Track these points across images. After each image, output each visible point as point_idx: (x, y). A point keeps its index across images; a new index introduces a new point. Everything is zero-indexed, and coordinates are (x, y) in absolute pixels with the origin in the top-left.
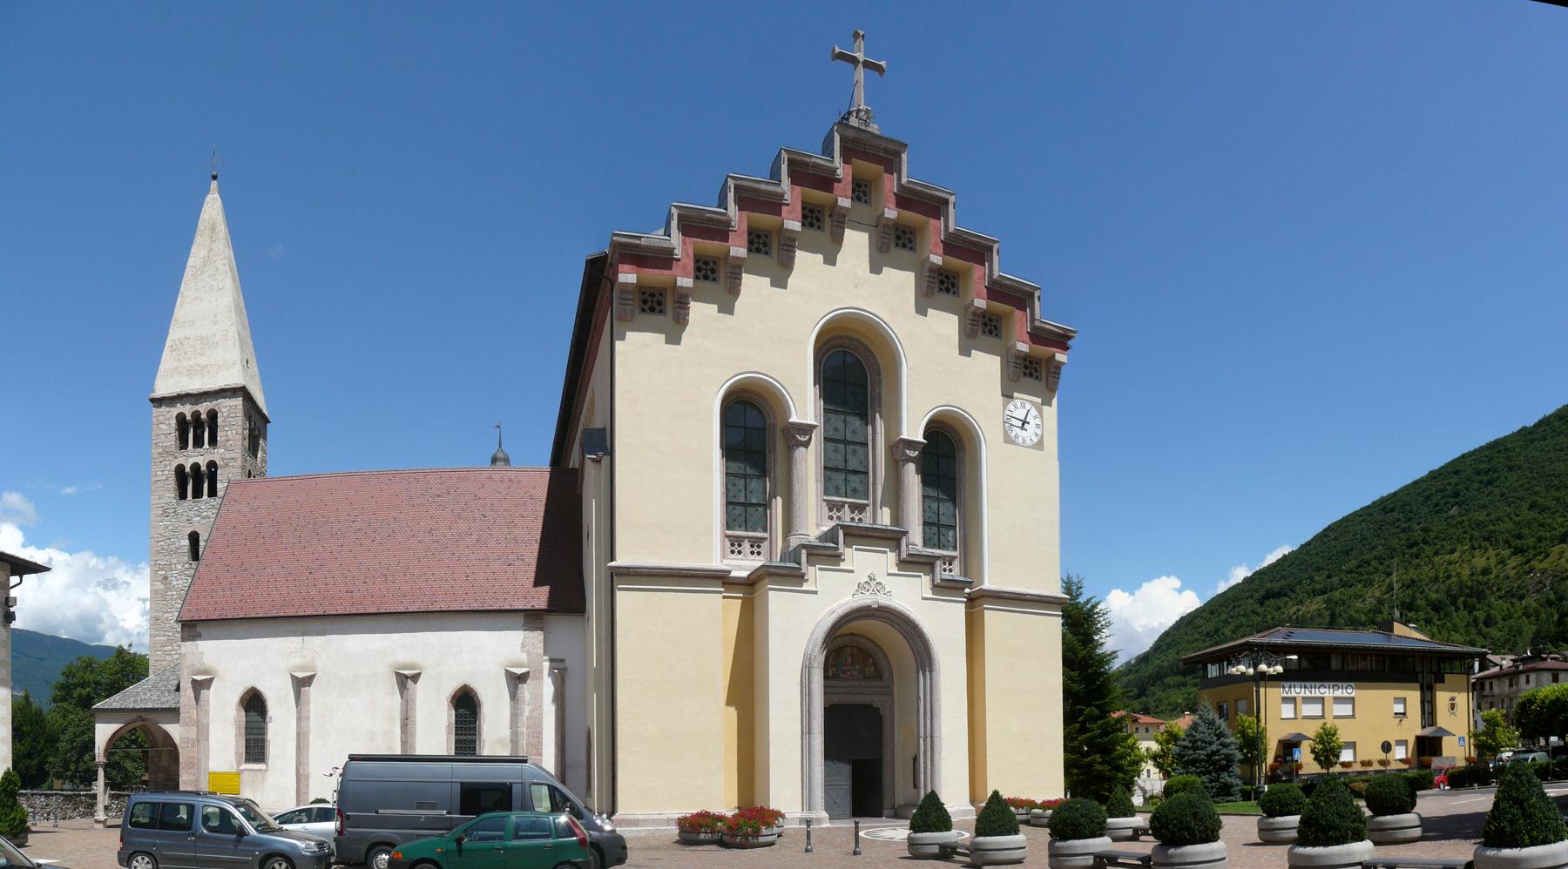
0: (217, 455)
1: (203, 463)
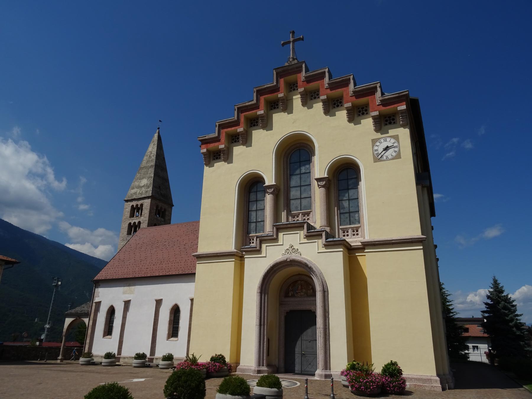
0: (141, 219)
1: (137, 221)
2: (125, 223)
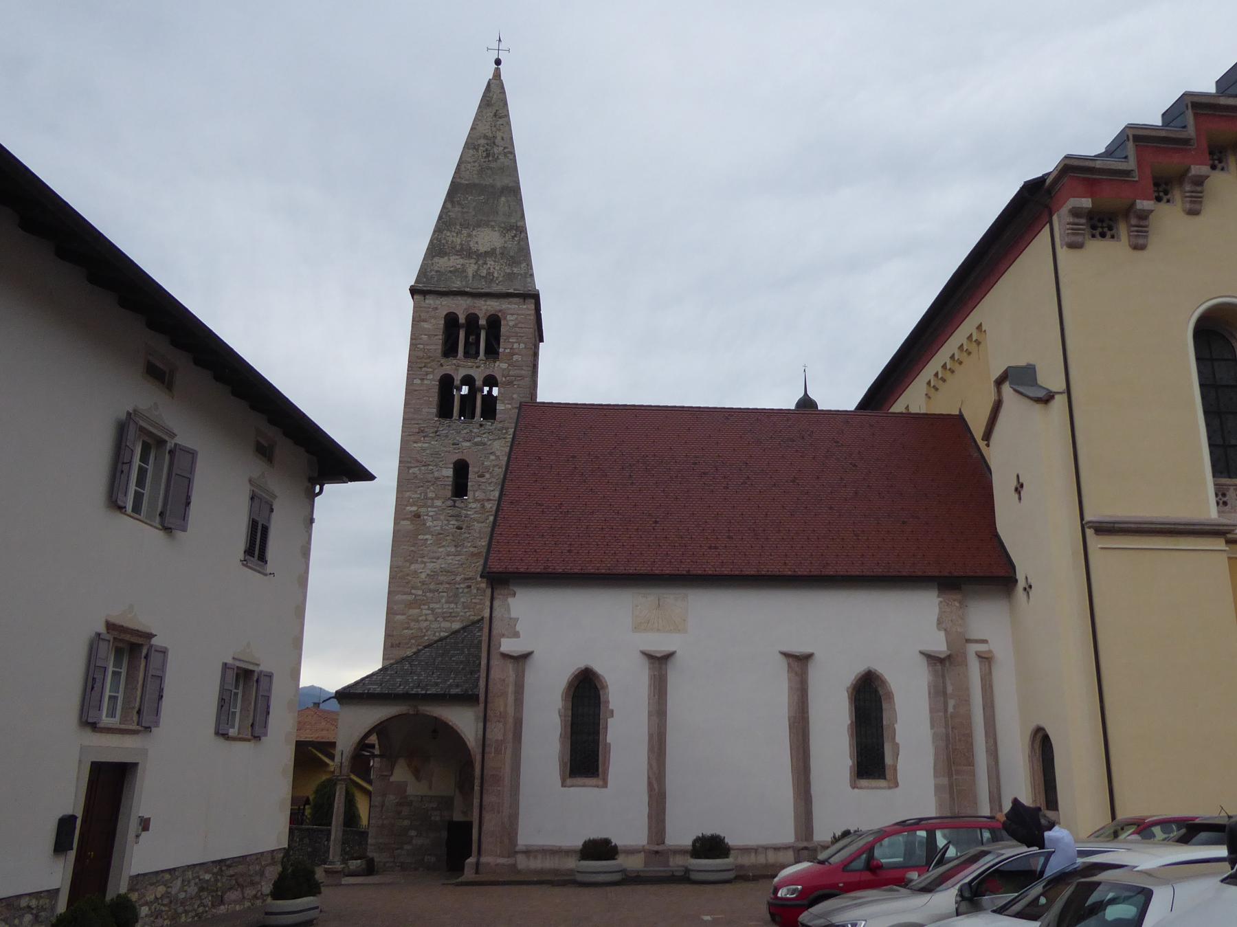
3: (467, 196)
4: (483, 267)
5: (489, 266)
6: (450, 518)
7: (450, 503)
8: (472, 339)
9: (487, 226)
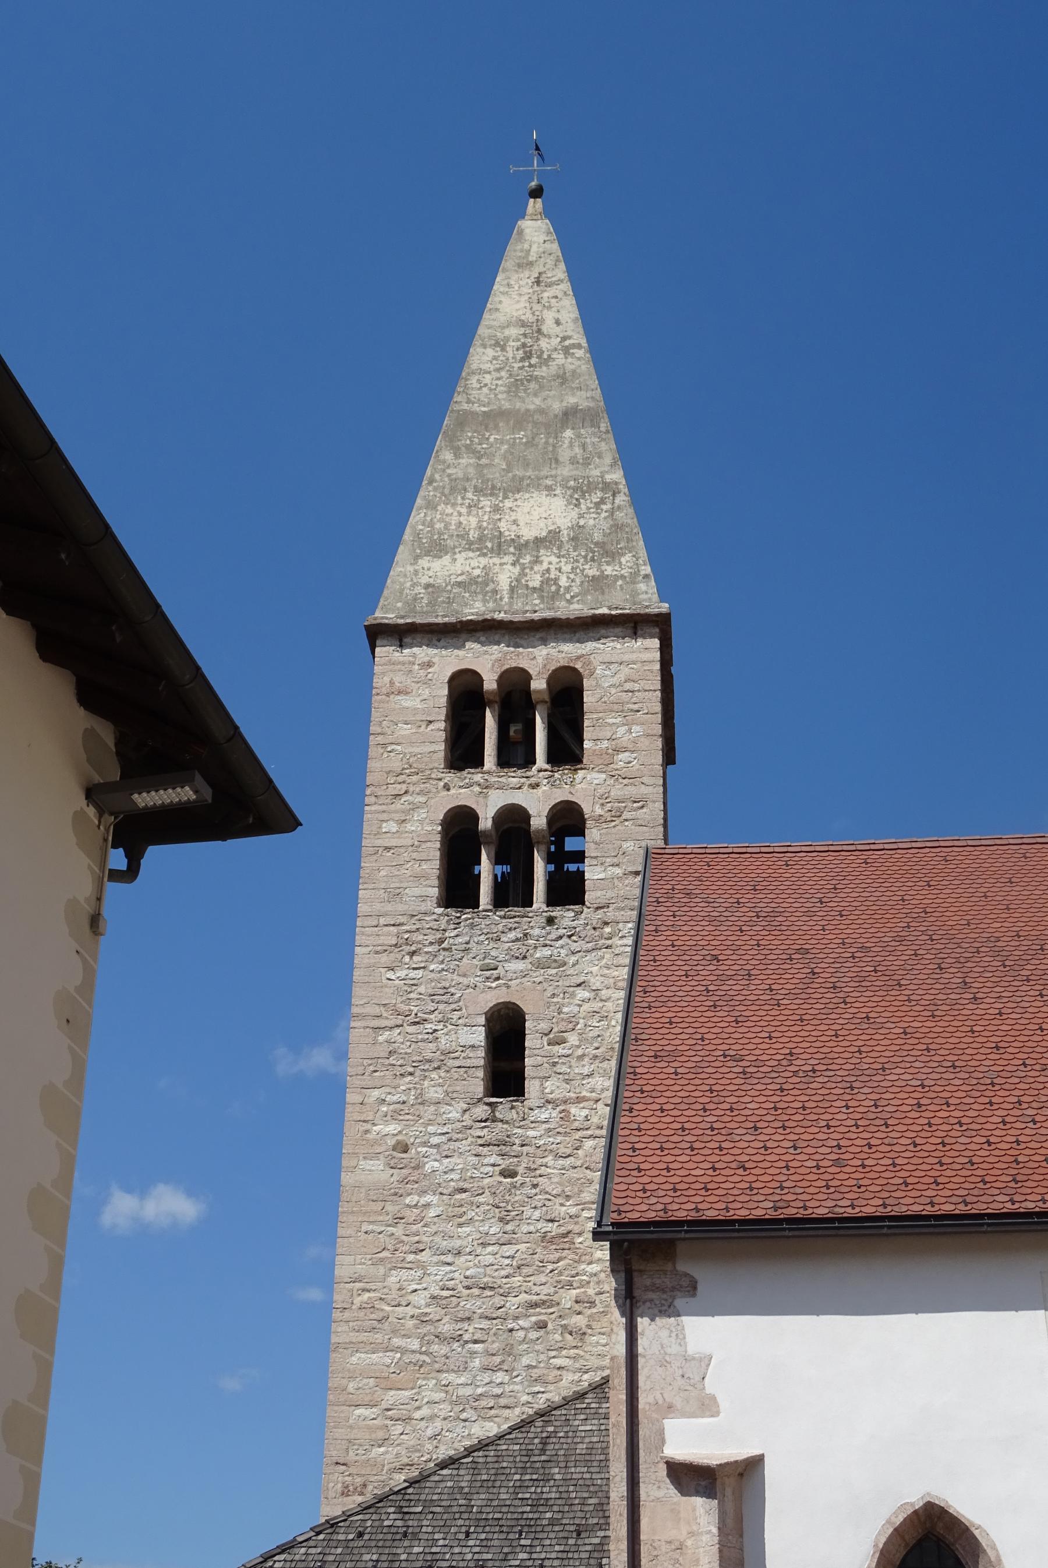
2: (398, 805)
3: (487, 434)
4: (532, 569)
5: (545, 566)
6: (485, 1150)
7: (481, 1111)
8: (514, 730)
9: (538, 487)
